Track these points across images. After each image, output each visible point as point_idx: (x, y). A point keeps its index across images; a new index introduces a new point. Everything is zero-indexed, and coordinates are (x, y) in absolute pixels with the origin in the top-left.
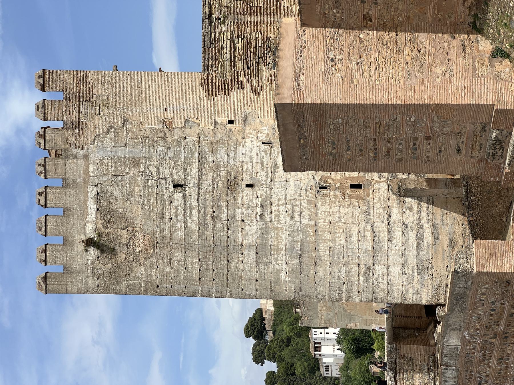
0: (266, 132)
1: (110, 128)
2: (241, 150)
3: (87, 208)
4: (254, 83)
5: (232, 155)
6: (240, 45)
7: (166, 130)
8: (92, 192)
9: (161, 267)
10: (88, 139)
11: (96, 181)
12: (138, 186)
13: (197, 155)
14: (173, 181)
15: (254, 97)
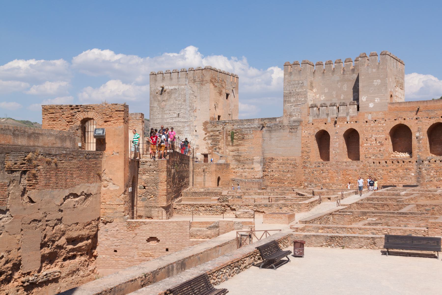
0: (193, 142)
1: (194, 92)
2: (188, 135)
3: (172, 86)
4: (207, 138)
5: (187, 132)
6: (217, 133)
7: (194, 110)
8: (176, 87)
9: (157, 111)
10: (191, 84)
11: (179, 88)
12: (178, 102)
13: (187, 121)
14: (180, 113)
15: (203, 138)
